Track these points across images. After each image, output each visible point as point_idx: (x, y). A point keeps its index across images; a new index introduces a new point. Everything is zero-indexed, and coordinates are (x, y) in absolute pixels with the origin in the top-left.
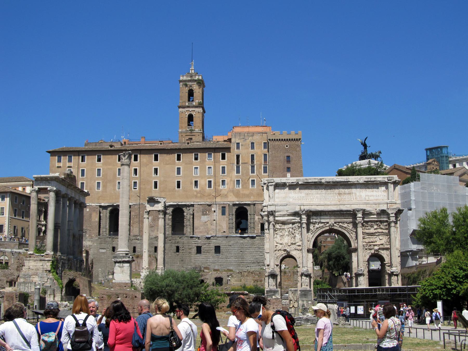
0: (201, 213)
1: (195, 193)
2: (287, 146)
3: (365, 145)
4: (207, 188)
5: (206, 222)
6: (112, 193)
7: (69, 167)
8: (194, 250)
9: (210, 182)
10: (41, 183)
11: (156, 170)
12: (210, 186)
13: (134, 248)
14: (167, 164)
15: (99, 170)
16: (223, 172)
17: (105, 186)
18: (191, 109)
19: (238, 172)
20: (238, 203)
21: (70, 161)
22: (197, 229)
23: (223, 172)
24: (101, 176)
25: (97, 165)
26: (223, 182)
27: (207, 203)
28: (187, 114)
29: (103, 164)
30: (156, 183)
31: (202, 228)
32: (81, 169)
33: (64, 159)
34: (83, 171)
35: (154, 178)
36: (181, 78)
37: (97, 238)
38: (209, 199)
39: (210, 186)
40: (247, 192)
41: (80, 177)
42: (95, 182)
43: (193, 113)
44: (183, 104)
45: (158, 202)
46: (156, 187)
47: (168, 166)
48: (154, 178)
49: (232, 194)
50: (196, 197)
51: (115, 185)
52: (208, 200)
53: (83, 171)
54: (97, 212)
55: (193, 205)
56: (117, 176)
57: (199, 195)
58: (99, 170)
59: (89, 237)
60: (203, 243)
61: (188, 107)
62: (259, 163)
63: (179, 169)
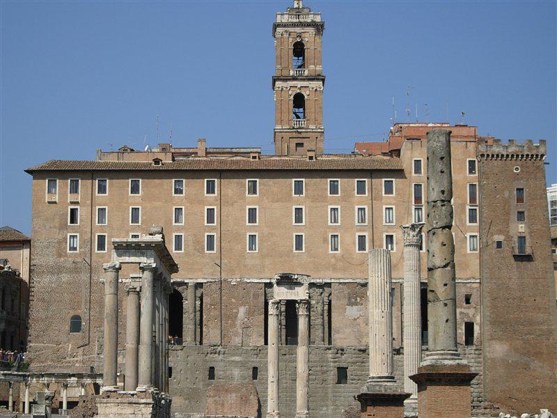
0: (346, 301)
2: (517, 169)
4: (357, 251)
5: (355, 319)
7: (72, 203)
8: (332, 375)
9: (362, 238)
10: (125, 253)
11: (252, 212)
13: (212, 369)
15: (135, 210)
18: (299, 84)
21: (74, 190)
22: (338, 332)
27: (358, 281)
28: (293, 92)
31: (348, 330)
32: (97, 207)
33: (63, 185)
34: (102, 211)
35: (249, 229)
36: (279, 19)
41: (97, 224)
43: (305, 93)
44: (285, 73)
45: (300, 284)
47: (276, 204)
53: (102, 211)
55: (329, 285)
56: (174, 224)
57: (340, 264)
58: (135, 210)
60: (350, 360)
61: (294, 79)
62: (460, 202)
63: (299, 211)
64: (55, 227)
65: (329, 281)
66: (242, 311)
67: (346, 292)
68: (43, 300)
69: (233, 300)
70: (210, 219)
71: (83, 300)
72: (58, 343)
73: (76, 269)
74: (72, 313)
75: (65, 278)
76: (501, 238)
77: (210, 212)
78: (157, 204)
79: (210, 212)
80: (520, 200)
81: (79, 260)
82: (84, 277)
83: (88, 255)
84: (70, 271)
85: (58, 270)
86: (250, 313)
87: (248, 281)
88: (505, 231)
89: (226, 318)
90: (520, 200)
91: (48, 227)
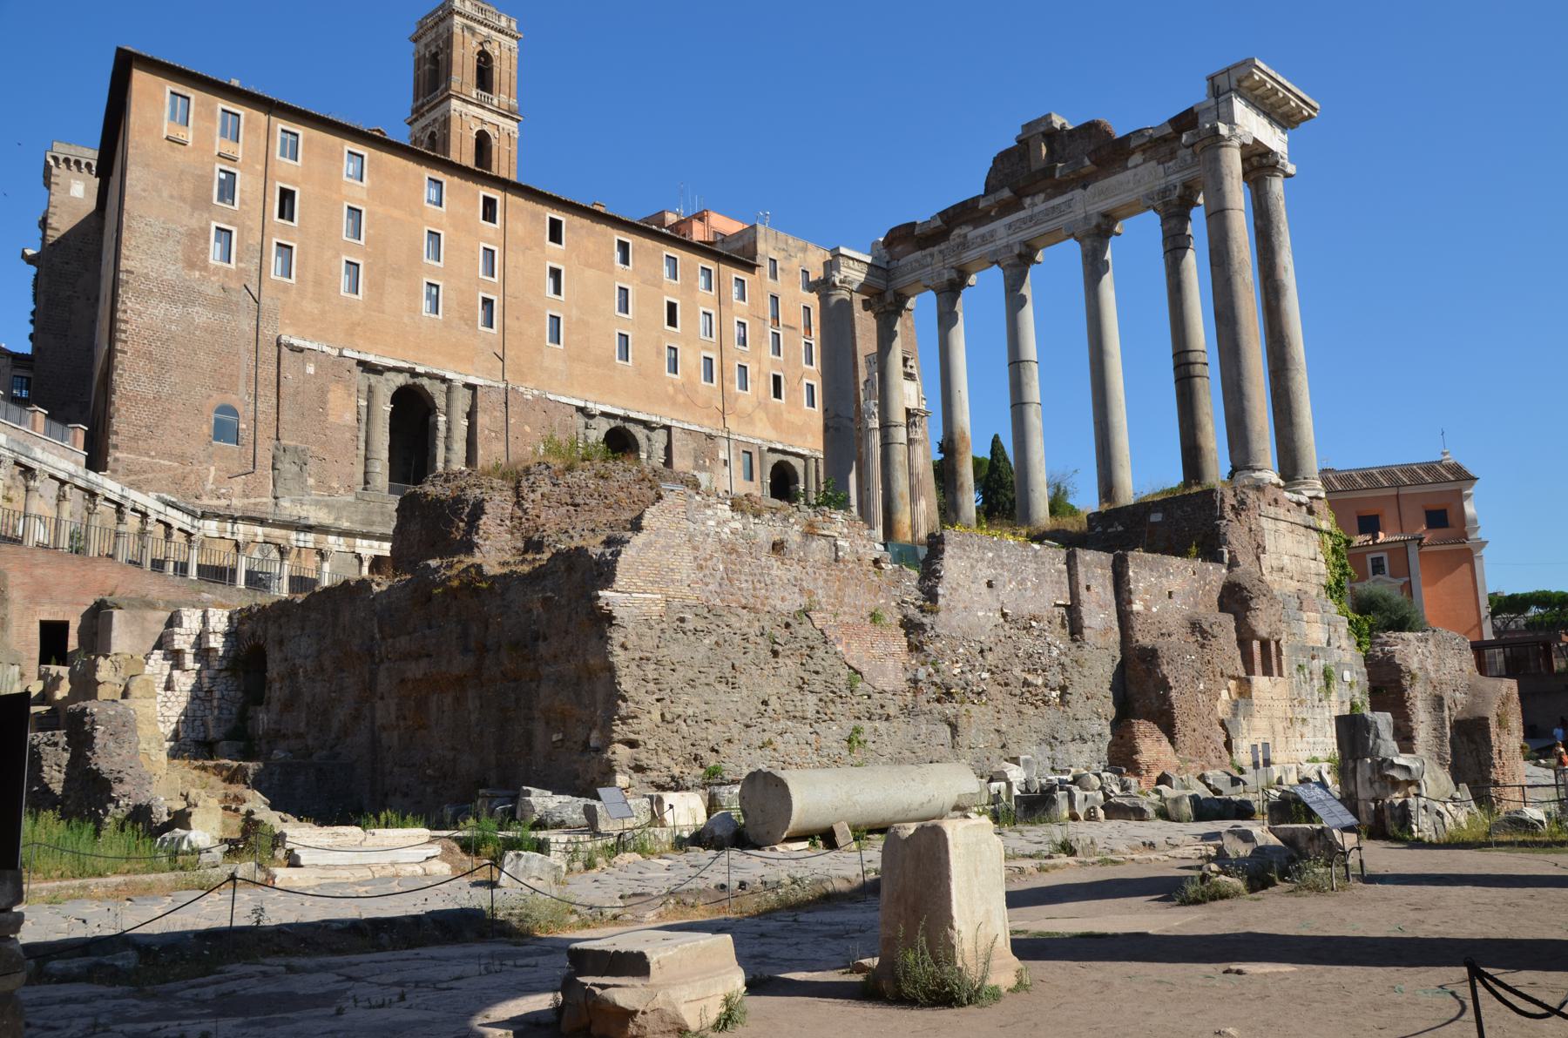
1: (671, 389)
6: (406, 320)
14: (590, 266)
17: (376, 287)
19: (777, 351)
20: (780, 447)
24: (362, 242)
25: (345, 190)
29: (369, 191)
35: (550, 303)
37: (351, 498)
38: (709, 417)
42: (338, 256)
47: (590, 273)
48: (550, 303)
49: (763, 415)
50: (673, 402)
51: (417, 294)
52: (706, 422)
54: (347, 387)
59: (317, 487)
64: (182, 199)
65: (668, 423)
67: (692, 445)
68: (149, 357)
69: (527, 429)
71: (243, 375)
72: (182, 458)
73: (224, 303)
74: (217, 399)
75: (202, 316)
78: (396, 213)
79: (489, 253)
81: (233, 284)
82: (246, 324)
83: (255, 279)
84: (213, 304)
85: (184, 295)
87: (551, 397)
91: (165, 194)
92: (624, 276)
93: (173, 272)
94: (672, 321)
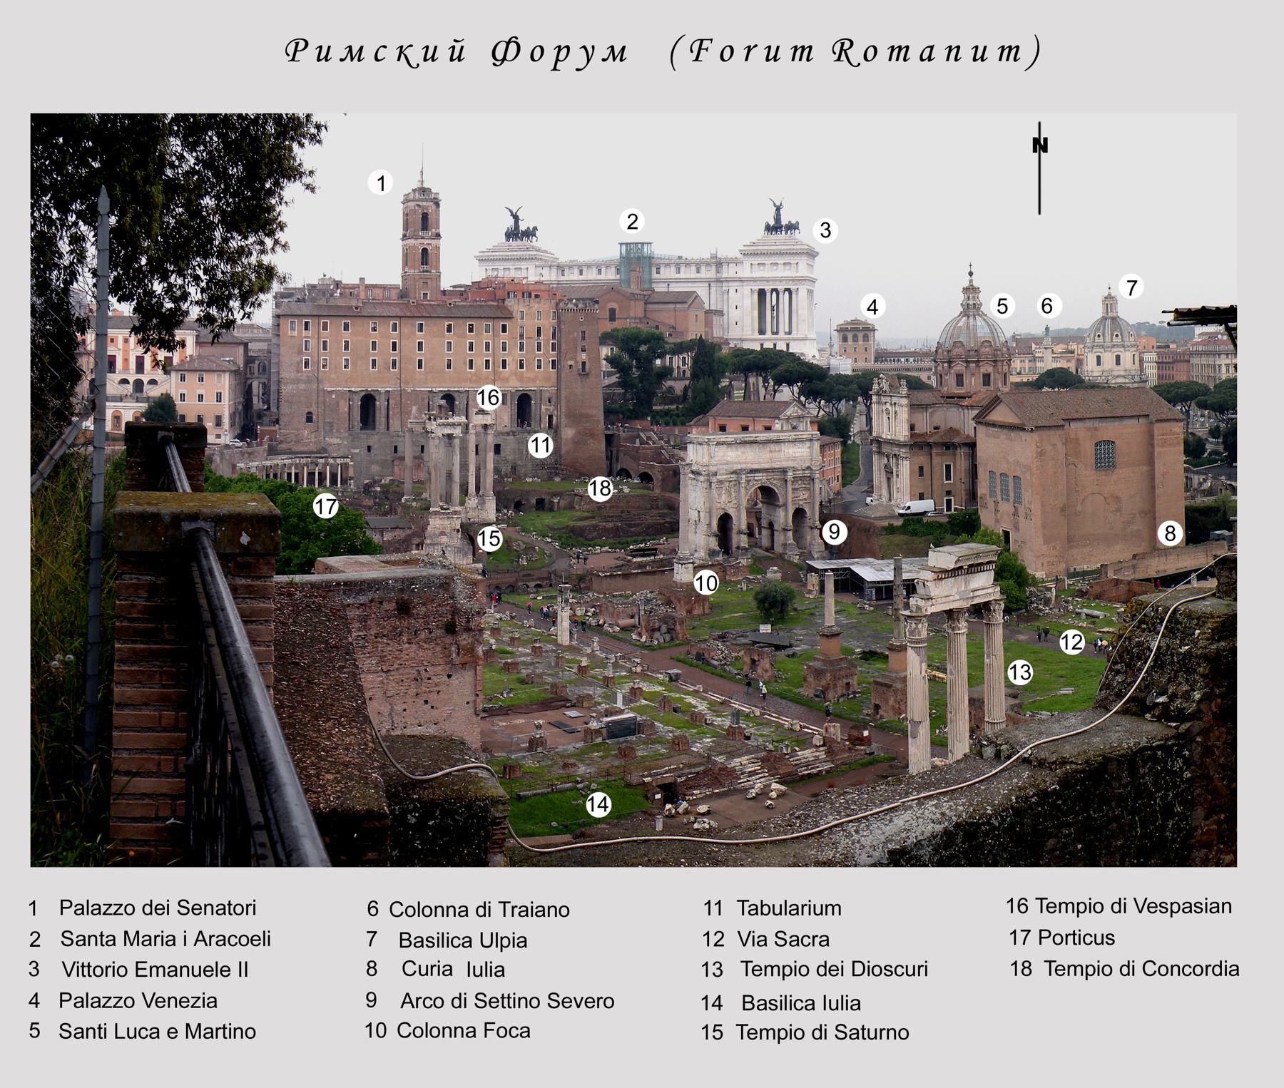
3: (516, 217)
9: (487, 361)
12: (487, 367)
15: (347, 343)
16: (504, 349)
23: (504, 349)
26: (504, 361)
30: (420, 361)
34: (325, 343)
39: (487, 367)
40: (531, 375)
43: (429, 248)
46: (420, 367)
48: (419, 355)
50: (470, 380)
53: (325, 343)
66: (414, 409)
70: (394, 349)
73: (309, 381)
76: (571, 363)
77: (394, 344)
79: (394, 344)
80: (583, 338)
82: (315, 386)
84: (305, 382)
85: (297, 381)
86: (419, 411)
88: (574, 358)
89: (404, 413)
90: (583, 338)
92: (450, 337)
93: (293, 375)
94: (471, 349)
